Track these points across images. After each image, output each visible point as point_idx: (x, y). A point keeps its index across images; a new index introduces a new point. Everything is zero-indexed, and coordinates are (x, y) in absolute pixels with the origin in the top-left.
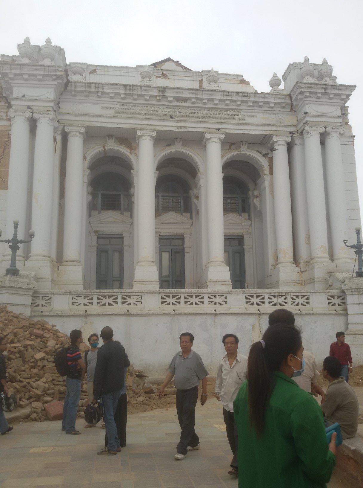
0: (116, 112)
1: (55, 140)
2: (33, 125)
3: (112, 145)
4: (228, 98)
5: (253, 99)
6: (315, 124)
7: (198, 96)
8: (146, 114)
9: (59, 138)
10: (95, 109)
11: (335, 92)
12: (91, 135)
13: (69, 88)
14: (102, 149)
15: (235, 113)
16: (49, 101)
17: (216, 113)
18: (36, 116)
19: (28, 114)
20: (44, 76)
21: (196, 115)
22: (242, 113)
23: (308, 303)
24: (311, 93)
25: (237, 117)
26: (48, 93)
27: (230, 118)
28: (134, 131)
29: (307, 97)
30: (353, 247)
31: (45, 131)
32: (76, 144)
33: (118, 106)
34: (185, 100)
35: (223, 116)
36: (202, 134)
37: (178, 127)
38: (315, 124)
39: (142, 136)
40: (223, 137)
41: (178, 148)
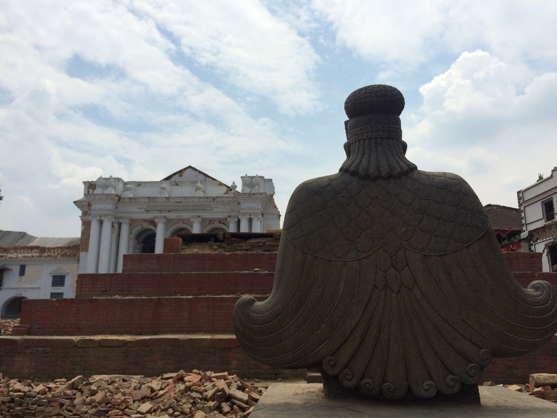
1: (113, 226)
2: (101, 222)
3: (146, 226)
4: (202, 200)
6: (245, 214)
9: (116, 225)
11: (255, 196)
12: (132, 223)
13: (121, 200)
14: (140, 227)
16: (109, 210)
18: (102, 218)
19: (98, 218)
26: (109, 206)
31: (107, 226)
32: (125, 228)
34: (181, 202)
36: (189, 219)
38: (245, 214)
41: (181, 225)
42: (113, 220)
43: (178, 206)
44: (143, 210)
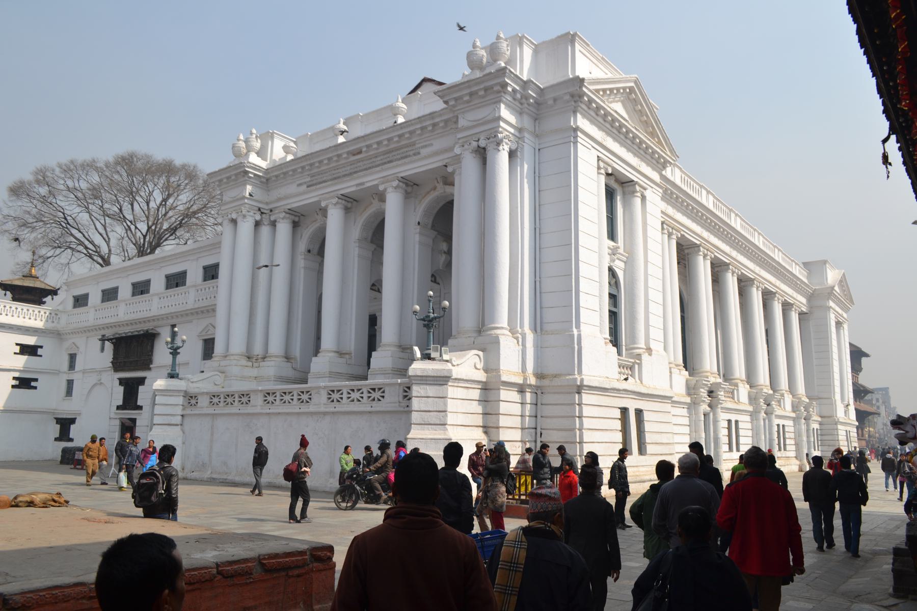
0: (308, 187)
5: (419, 126)
7: (368, 143)
8: (331, 180)
10: (292, 189)
15: (410, 148)
17: (391, 155)
18: (234, 216)
20: (236, 175)
21: (373, 164)
22: (417, 146)
23: (383, 397)
24: (456, 99)
25: (411, 153)
27: (406, 157)
28: (319, 202)
29: (454, 106)
30: (423, 320)
33: (309, 179)
35: (398, 157)
37: (357, 185)
39: (327, 206)
40: (395, 183)
42: (258, 217)
43: (359, 161)
44: (304, 187)
